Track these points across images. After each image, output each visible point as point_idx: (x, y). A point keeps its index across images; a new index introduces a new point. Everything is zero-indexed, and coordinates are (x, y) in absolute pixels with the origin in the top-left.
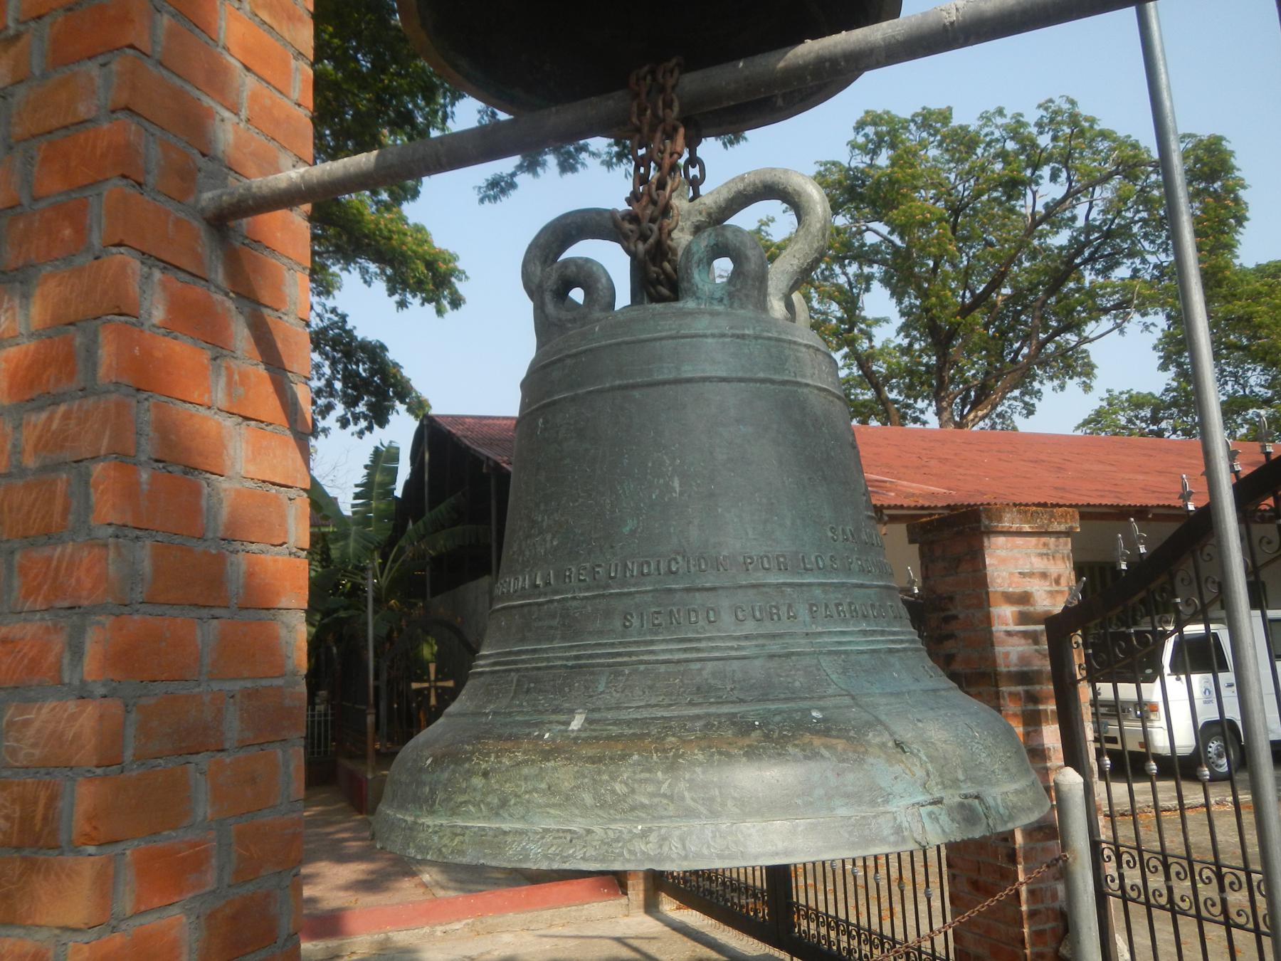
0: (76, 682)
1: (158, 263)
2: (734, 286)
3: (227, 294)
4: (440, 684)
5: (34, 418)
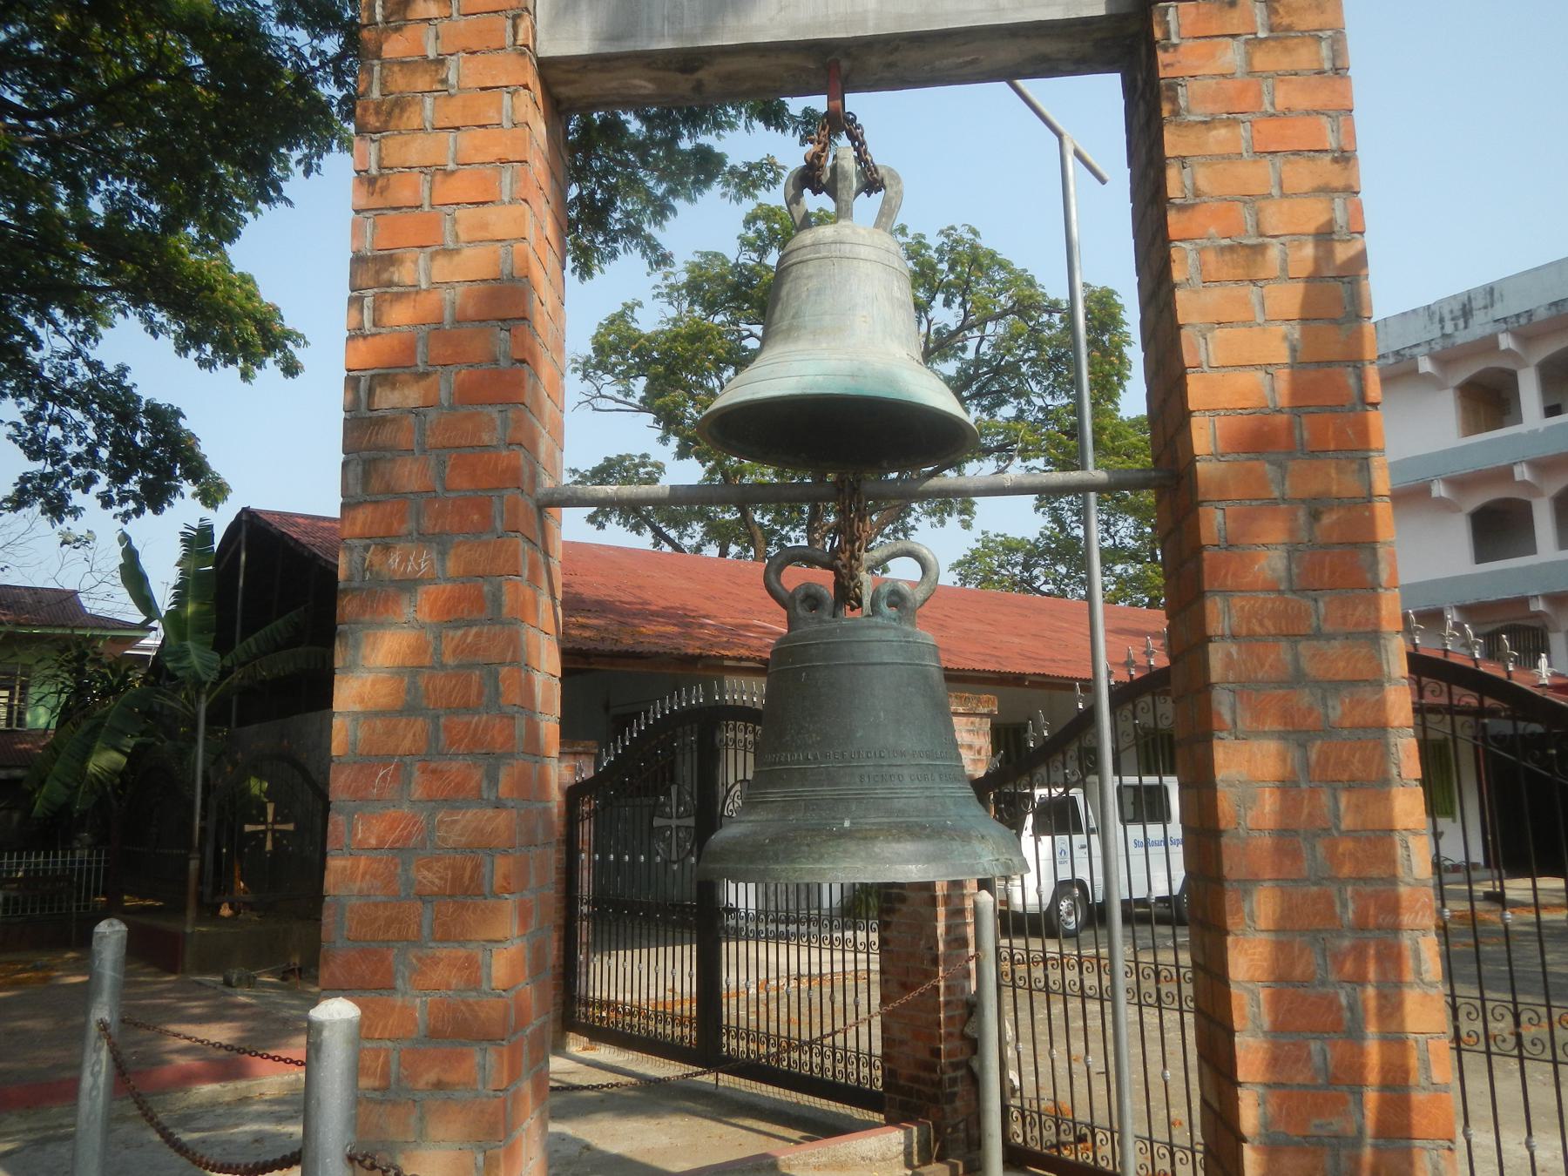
0: (493, 798)
4: (277, 827)
5: (451, 633)
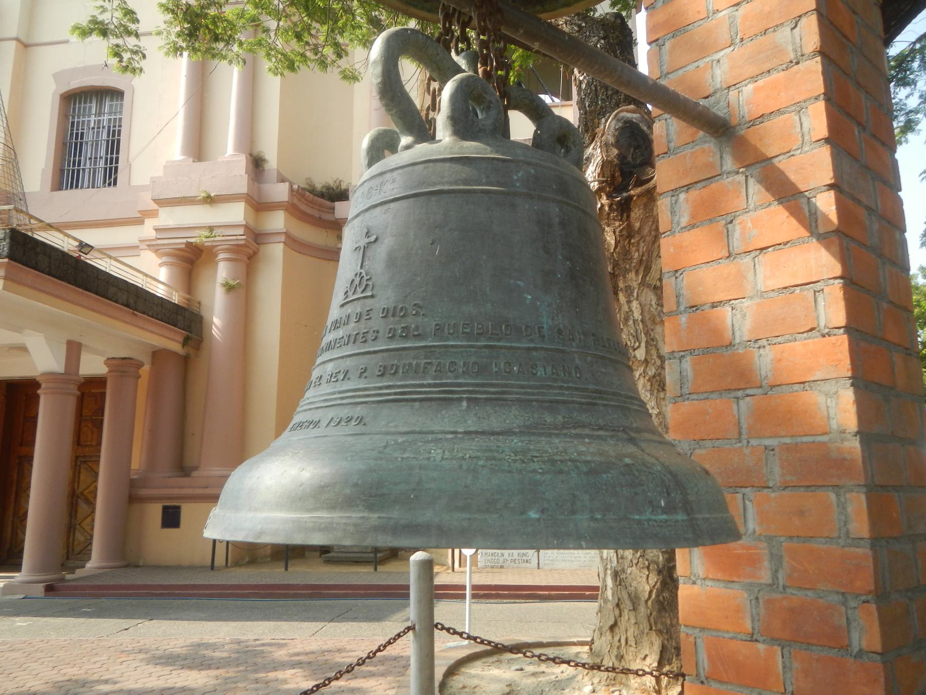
1: (683, 189)
3: (738, 173)
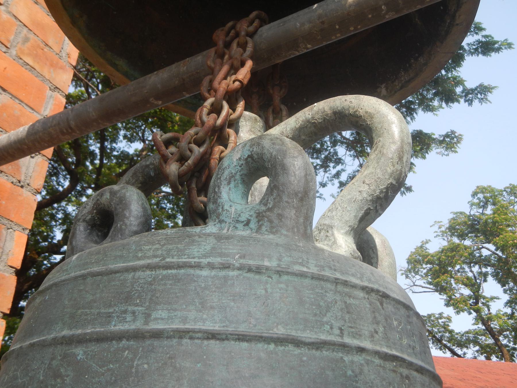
2: (265, 205)
